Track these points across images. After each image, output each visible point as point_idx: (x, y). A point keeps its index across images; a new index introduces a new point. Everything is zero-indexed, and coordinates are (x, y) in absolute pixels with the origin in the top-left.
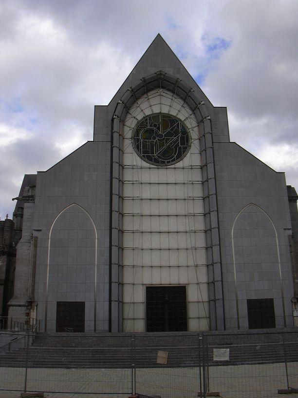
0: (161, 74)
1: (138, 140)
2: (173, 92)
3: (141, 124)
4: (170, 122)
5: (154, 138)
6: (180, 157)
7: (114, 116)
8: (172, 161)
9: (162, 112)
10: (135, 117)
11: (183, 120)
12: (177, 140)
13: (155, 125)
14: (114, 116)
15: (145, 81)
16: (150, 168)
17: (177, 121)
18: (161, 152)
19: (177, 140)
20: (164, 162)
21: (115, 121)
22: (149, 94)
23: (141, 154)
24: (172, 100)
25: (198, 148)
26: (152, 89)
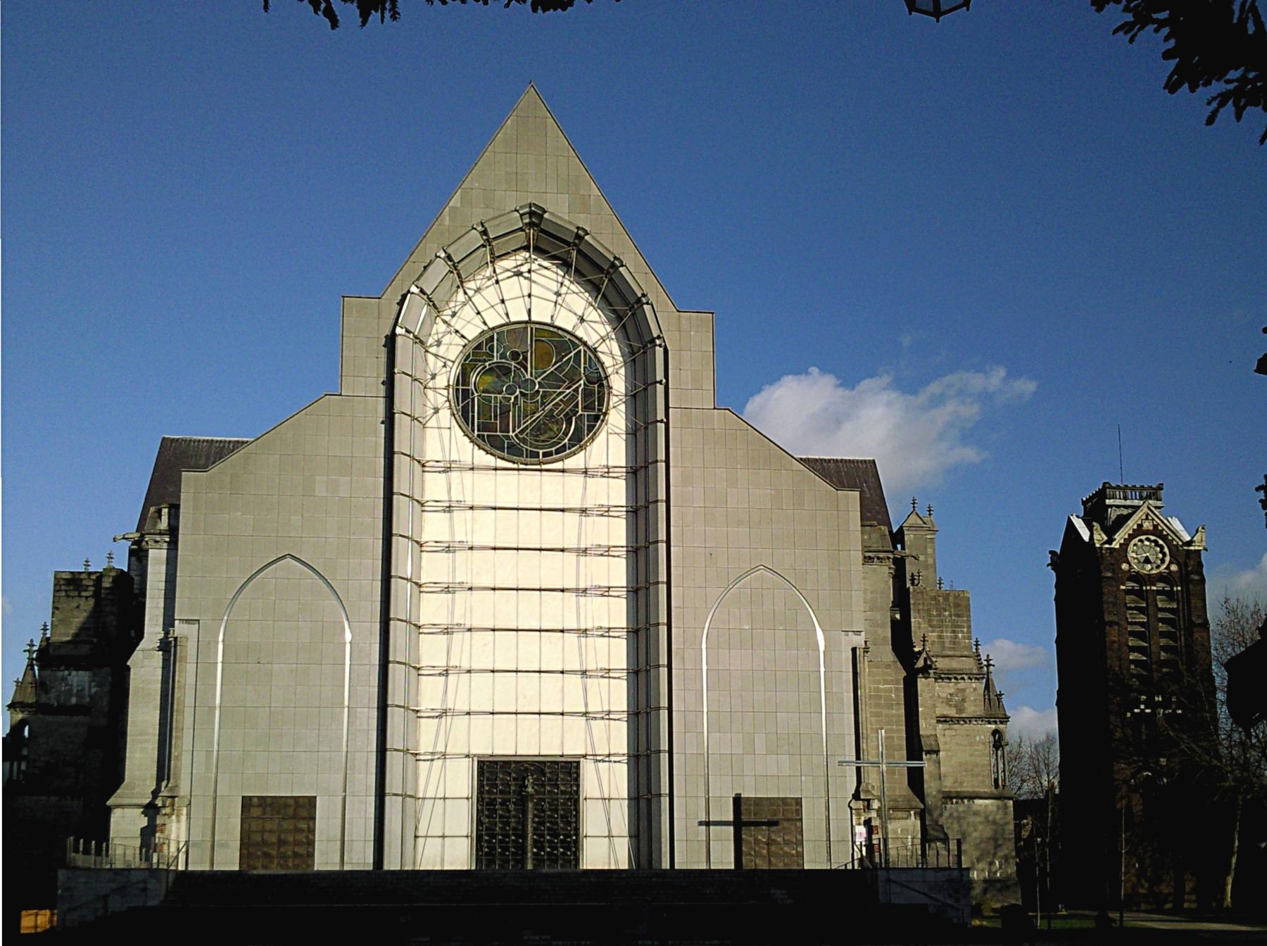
1: (466, 393)
2: (565, 264)
3: (477, 354)
4: (556, 348)
5: (511, 391)
6: (579, 441)
8: (557, 452)
9: (534, 318)
12: (574, 397)
13: (515, 356)
16: (496, 469)
18: (527, 427)
19: (574, 397)
20: (537, 455)
23: (473, 431)
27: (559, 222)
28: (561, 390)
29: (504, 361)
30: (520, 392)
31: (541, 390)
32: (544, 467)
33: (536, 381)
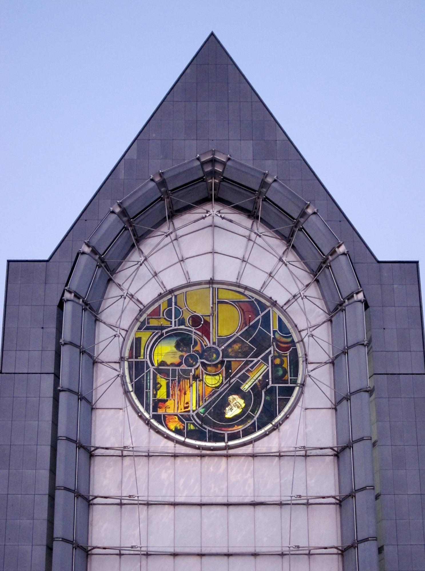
0: (213, 161)
2: (252, 214)
7: (67, 296)
8: (246, 433)
10: (132, 296)
11: (281, 302)
14: (67, 296)
15: (163, 183)
16: (175, 456)
17: (263, 307)
21: (68, 307)
22: (178, 222)
24: (249, 239)
25: (329, 392)
26: (187, 208)
27: (243, 169)
28: (248, 359)
29: (182, 327)
30: (202, 363)
31: (226, 360)
32: (231, 452)
33: (220, 350)
